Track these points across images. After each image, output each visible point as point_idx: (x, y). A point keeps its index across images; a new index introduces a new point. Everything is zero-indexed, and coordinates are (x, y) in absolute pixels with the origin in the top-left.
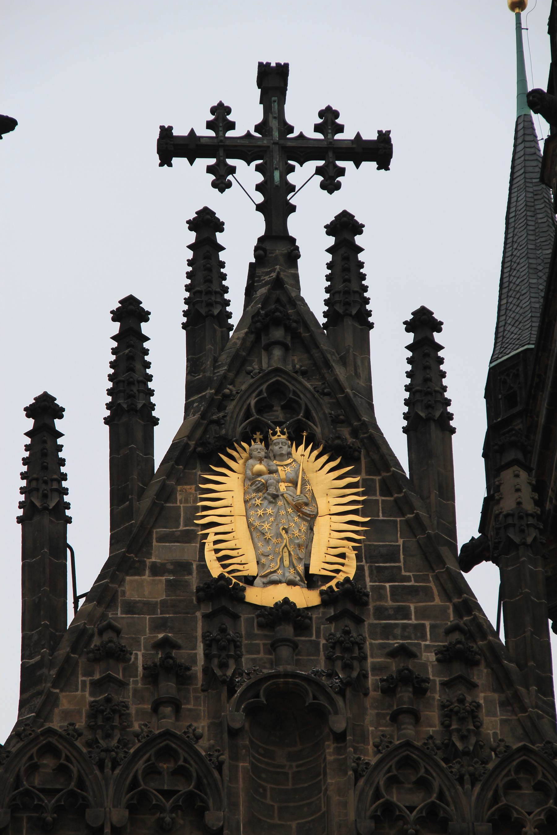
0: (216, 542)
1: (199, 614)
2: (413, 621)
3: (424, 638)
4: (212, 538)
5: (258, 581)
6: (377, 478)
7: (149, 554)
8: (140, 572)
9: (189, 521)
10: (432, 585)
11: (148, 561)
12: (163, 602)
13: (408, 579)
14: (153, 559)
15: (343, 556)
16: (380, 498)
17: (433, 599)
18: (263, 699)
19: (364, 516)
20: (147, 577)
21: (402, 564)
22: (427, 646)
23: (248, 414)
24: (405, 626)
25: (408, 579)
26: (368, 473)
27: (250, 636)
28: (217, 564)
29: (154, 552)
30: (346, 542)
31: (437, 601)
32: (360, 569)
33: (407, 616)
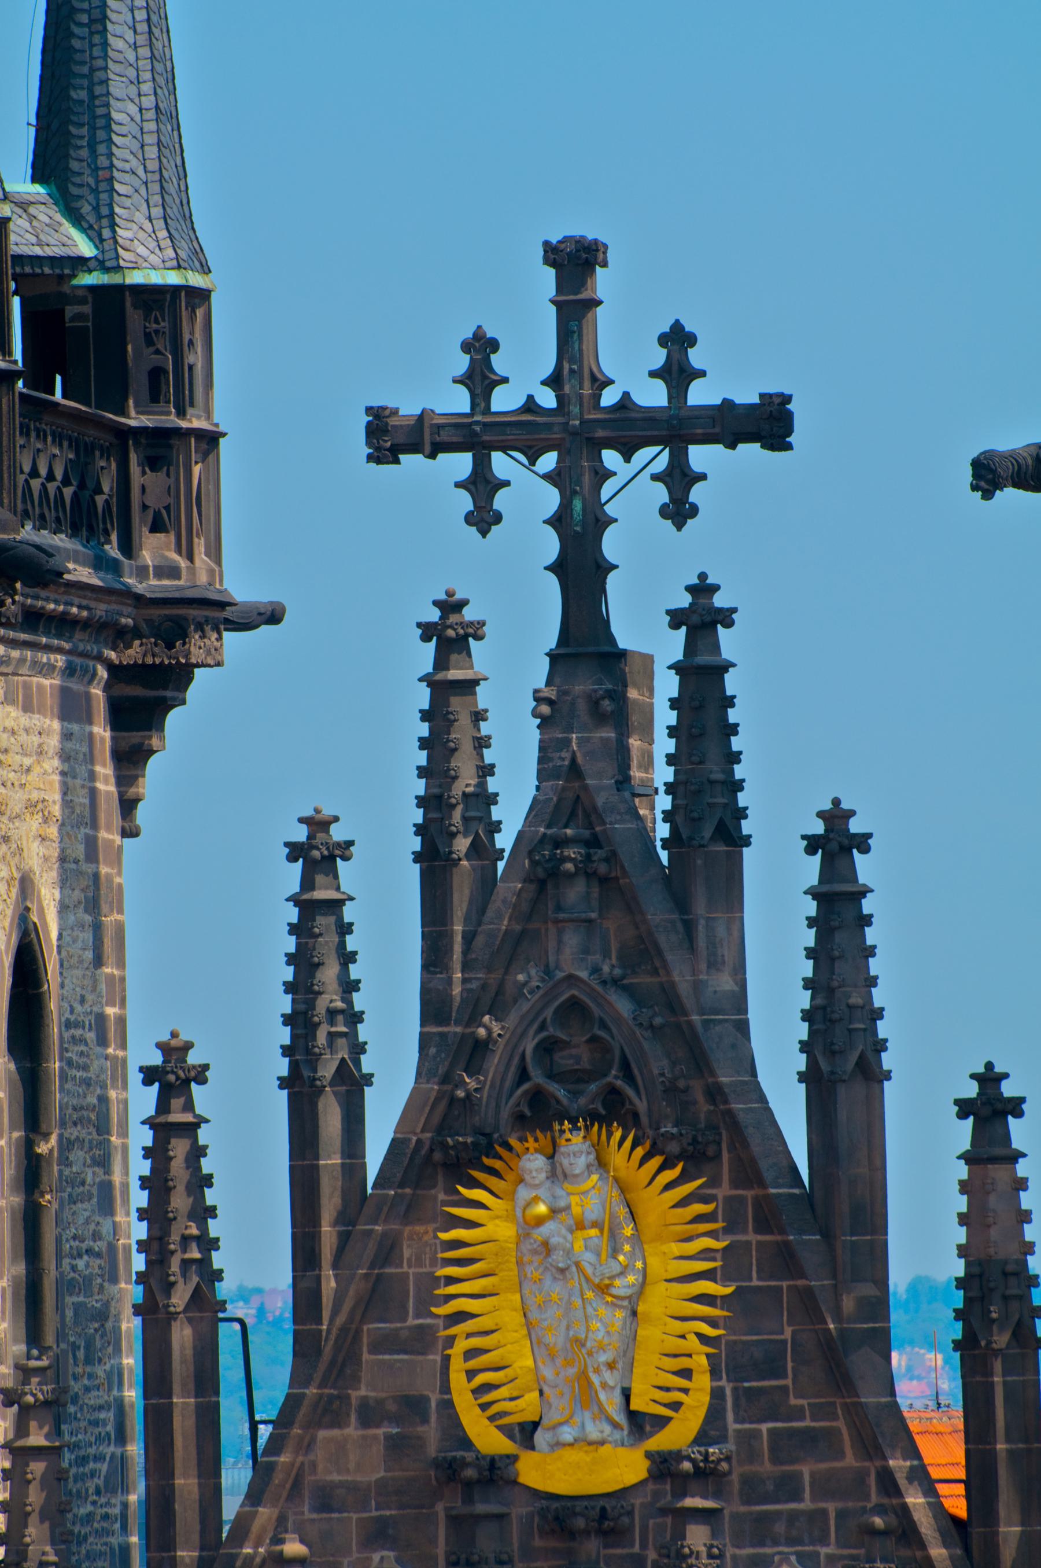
2: (807, 1504)
3: (824, 1541)
6: (749, 1194)
8: (338, 1421)
10: (841, 1424)
11: (355, 1395)
12: (381, 1483)
13: (798, 1414)
14: (363, 1392)
16: (752, 1237)
17: (841, 1455)
19: (726, 1280)
20: (352, 1431)
21: (789, 1382)
23: (523, 1075)
24: (793, 1517)
25: (798, 1414)
26: (735, 1184)
29: (365, 1375)
31: (850, 1460)
32: (717, 1394)
33: (796, 1495)
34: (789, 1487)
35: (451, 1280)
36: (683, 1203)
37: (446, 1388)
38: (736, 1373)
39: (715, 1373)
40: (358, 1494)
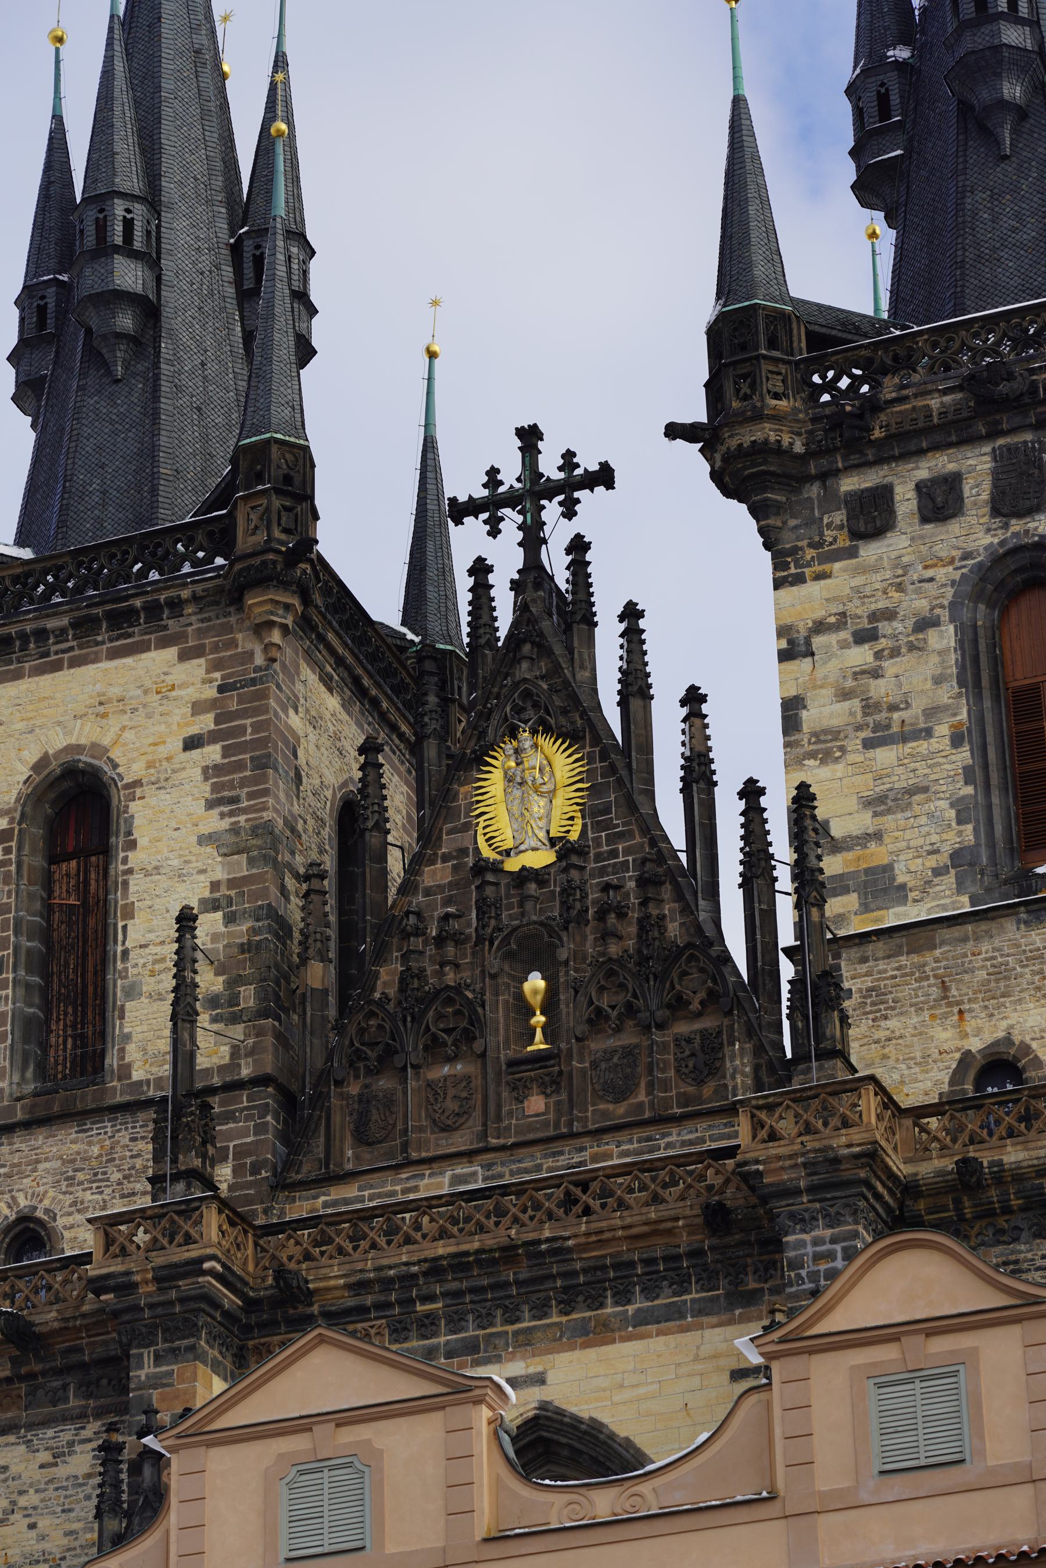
0: (484, 828)
1: (473, 887)
4: (482, 824)
5: (512, 853)
7: (440, 847)
8: (432, 862)
9: (467, 815)
10: (634, 827)
12: (450, 883)
13: (617, 826)
15: (572, 818)
16: (598, 765)
18: (514, 946)
21: (613, 815)
22: (630, 877)
24: (615, 864)
25: (617, 826)
26: (591, 746)
27: (508, 896)
28: (486, 844)
30: (575, 807)
31: (638, 839)
32: (584, 825)
34: (614, 854)
35: (478, 802)
36: (569, 756)
37: (476, 843)
38: (593, 815)
39: (583, 817)
40: (440, 888)
